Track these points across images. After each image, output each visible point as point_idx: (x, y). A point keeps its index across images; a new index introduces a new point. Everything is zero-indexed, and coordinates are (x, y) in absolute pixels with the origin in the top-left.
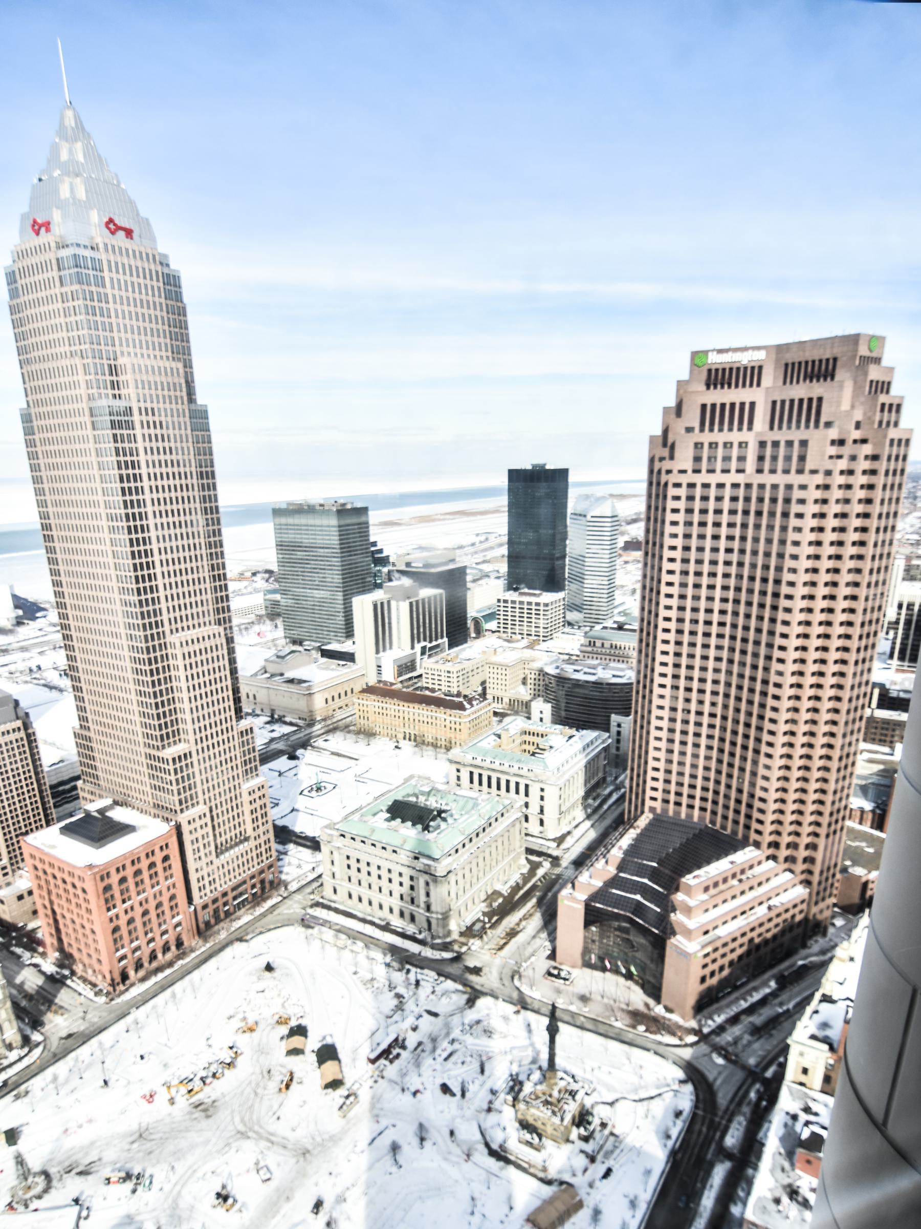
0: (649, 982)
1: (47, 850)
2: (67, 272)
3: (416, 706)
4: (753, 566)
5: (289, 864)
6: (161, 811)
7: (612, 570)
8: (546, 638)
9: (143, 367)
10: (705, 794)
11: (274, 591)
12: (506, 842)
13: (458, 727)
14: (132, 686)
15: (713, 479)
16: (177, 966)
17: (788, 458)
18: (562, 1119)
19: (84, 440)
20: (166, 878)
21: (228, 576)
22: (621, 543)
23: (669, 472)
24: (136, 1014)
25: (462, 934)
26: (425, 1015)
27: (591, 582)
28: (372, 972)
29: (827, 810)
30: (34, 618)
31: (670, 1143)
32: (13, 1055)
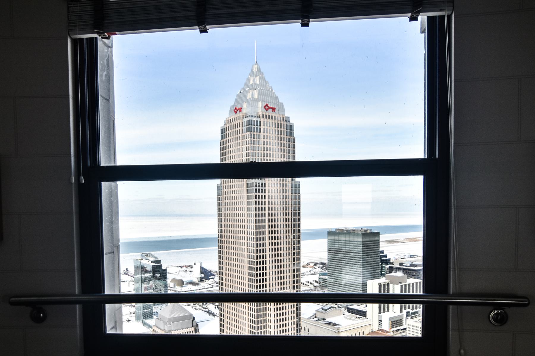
11: (325, 274)
14: (247, 316)
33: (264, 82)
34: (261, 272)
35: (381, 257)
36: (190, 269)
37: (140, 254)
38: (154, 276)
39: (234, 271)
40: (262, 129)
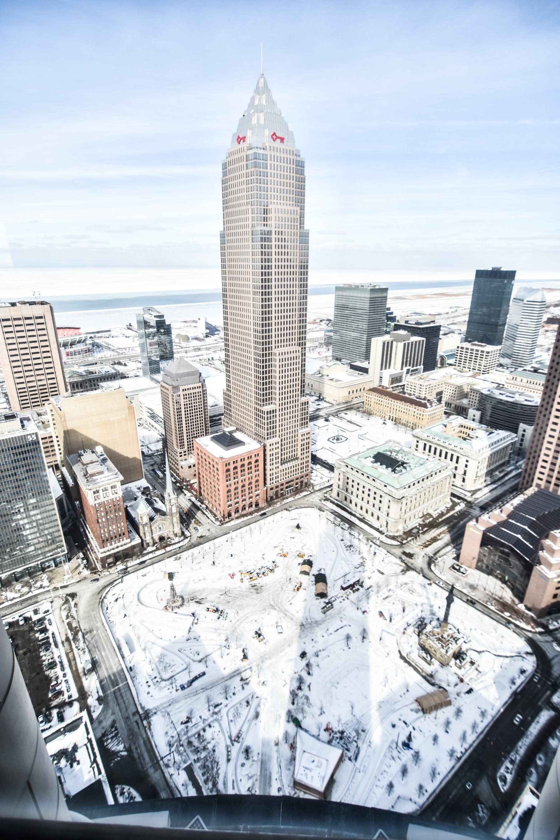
0: (517, 588)
1: (204, 447)
2: (250, 162)
3: (399, 402)
5: (317, 476)
6: (258, 437)
7: (535, 335)
8: (484, 372)
9: (280, 208)
11: (331, 331)
12: (440, 487)
13: (421, 417)
16: (254, 515)
18: (447, 652)
19: (247, 247)
20: (255, 471)
21: (308, 321)
22: (545, 318)
24: (233, 534)
25: (404, 533)
26: (377, 572)
27: (520, 341)
28: (351, 541)
30: (213, 334)
31: (514, 687)
32: (177, 539)
33: (271, 102)
34: (267, 334)
36: (194, 324)
37: (142, 308)
38: (158, 331)
39: (240, 327)
40: (269, 165)
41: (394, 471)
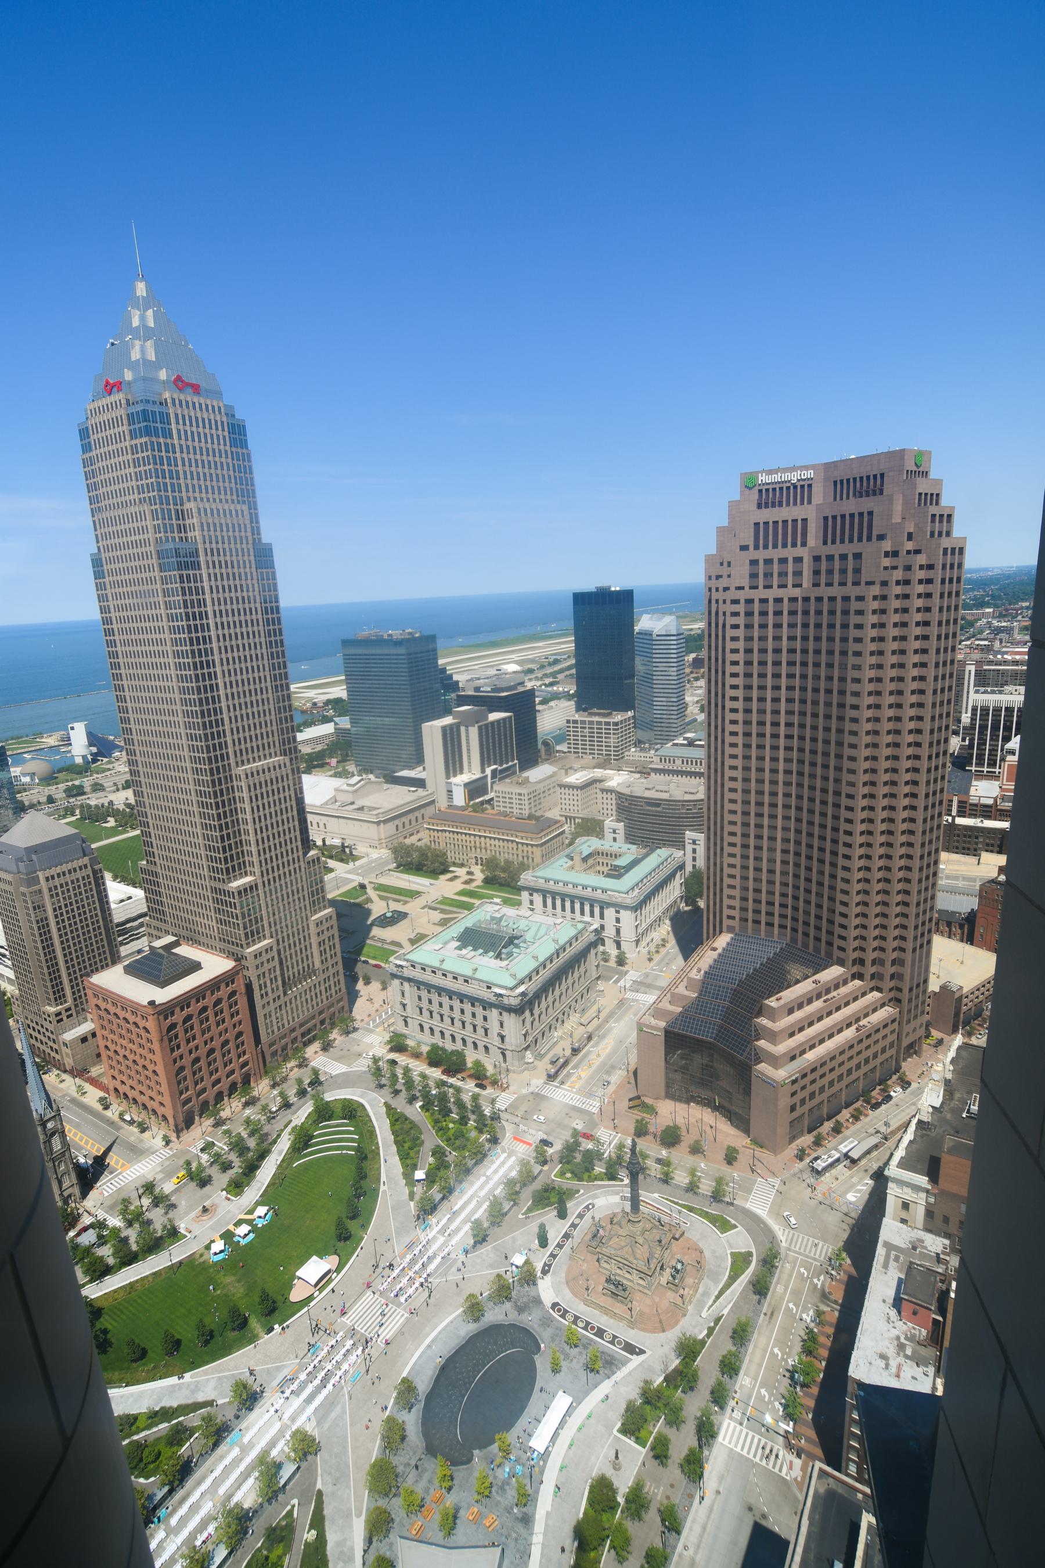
4: (817, 678)
10: (784, 911)
15: (771, 594)
17: (843, 571)
23: (726, 589)
29: (911, 922)
35: (442, 679)
39: (159, 734)
40: (175, 432)
41: (498, 956)
